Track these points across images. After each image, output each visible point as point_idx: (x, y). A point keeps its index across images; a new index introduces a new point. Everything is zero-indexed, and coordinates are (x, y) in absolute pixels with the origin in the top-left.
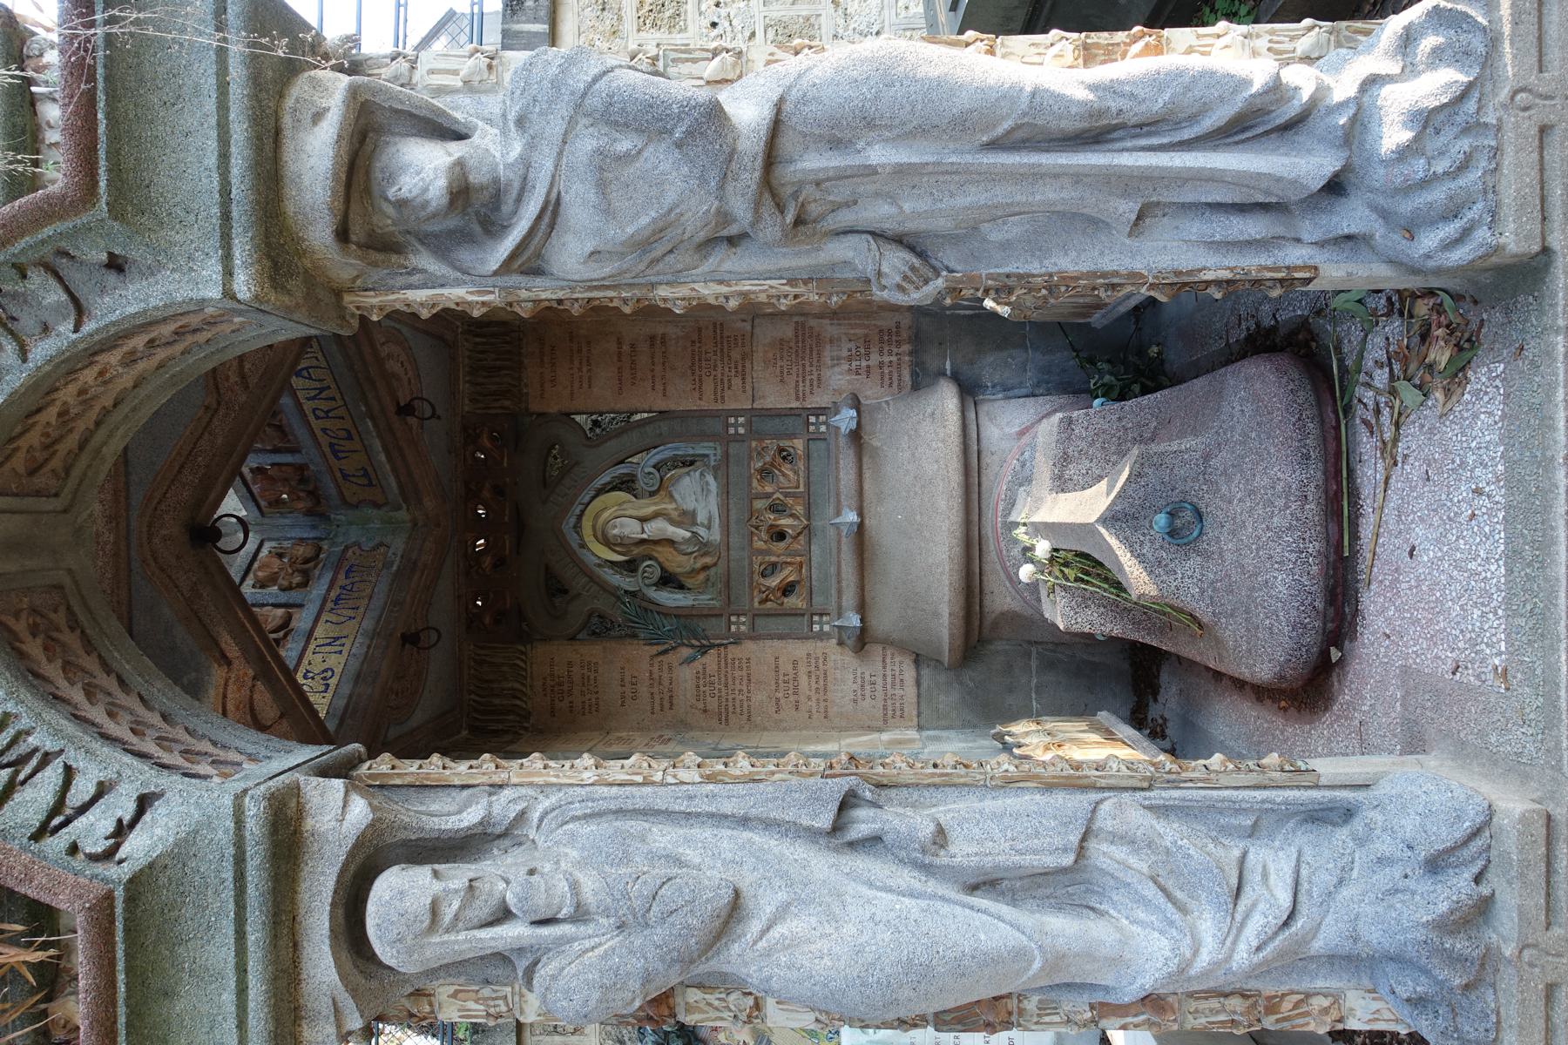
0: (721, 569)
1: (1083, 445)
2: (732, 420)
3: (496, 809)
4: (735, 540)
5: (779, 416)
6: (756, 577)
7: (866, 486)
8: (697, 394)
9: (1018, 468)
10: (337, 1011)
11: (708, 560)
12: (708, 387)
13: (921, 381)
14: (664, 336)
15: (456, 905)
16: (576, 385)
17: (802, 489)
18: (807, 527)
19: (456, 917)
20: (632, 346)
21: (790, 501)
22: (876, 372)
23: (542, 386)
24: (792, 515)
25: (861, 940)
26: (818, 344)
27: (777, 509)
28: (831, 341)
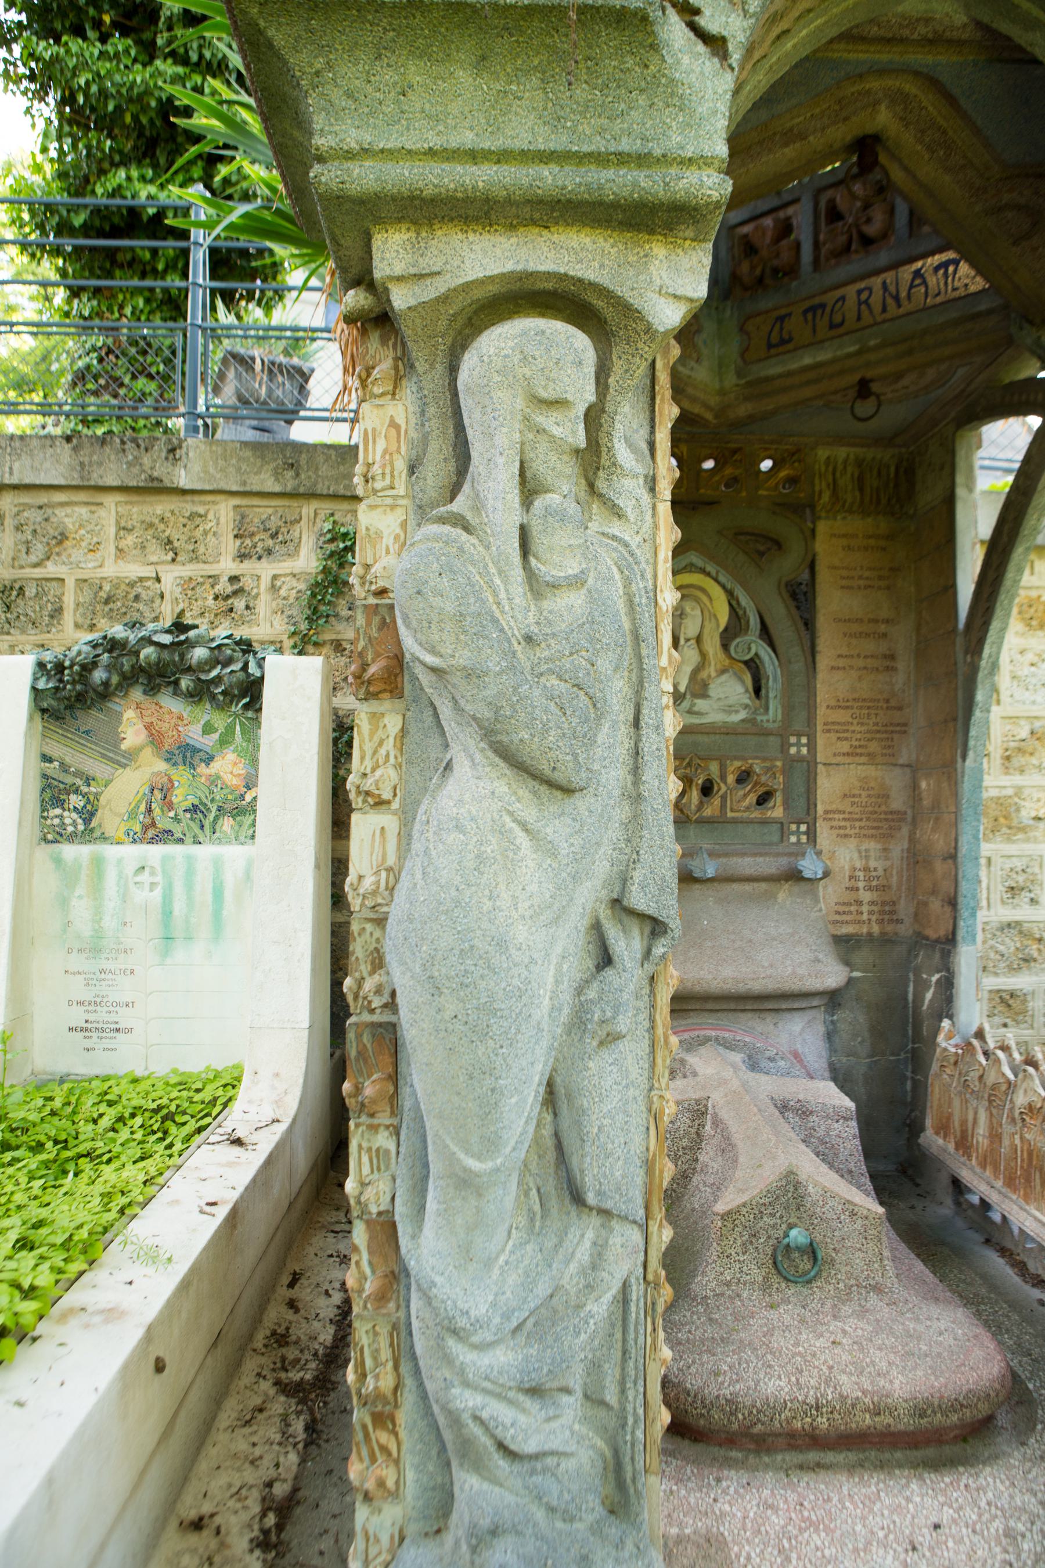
1: (821, 1132)
2: (804, 740)
3: (628, 483)
7: (736, 886)
8: (833, 703)
9: (768, 1054)
10: (420, 277)
13: (845, 945)
14: (894, 669)
15: (557, 431)
16: (845, 573)
17: (730, 814)
19: (540, 431)
20: (885, 635)
21: (717, 801)
22: (850, 897)
23: (844, 536)
24: (701, 803)
25: (511, 946)
26: (883, 836)
28: (885, 850)
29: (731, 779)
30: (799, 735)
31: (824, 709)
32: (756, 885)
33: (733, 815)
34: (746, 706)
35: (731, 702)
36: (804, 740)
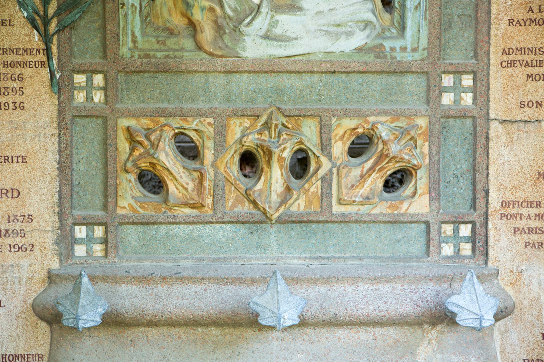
0: (191, 57)
2: (467, 81)
4: (244, 83)
5: (474, 168)
6: (176, 123)
7: (341, 332)
8: (521, 14)
11: (207, 34)
12: (531, 37)
17: (337, 209)
18: (266, 218)
21: (314, 186)
24: (288, 189)
27: (301, 165)
29: (339, 149)
30: (458, 73)
31: (504, 25)
32: (379, 331)
33: (343, 209)
34: (367, 24)
35: (338, 18)
36: (467, 81)
